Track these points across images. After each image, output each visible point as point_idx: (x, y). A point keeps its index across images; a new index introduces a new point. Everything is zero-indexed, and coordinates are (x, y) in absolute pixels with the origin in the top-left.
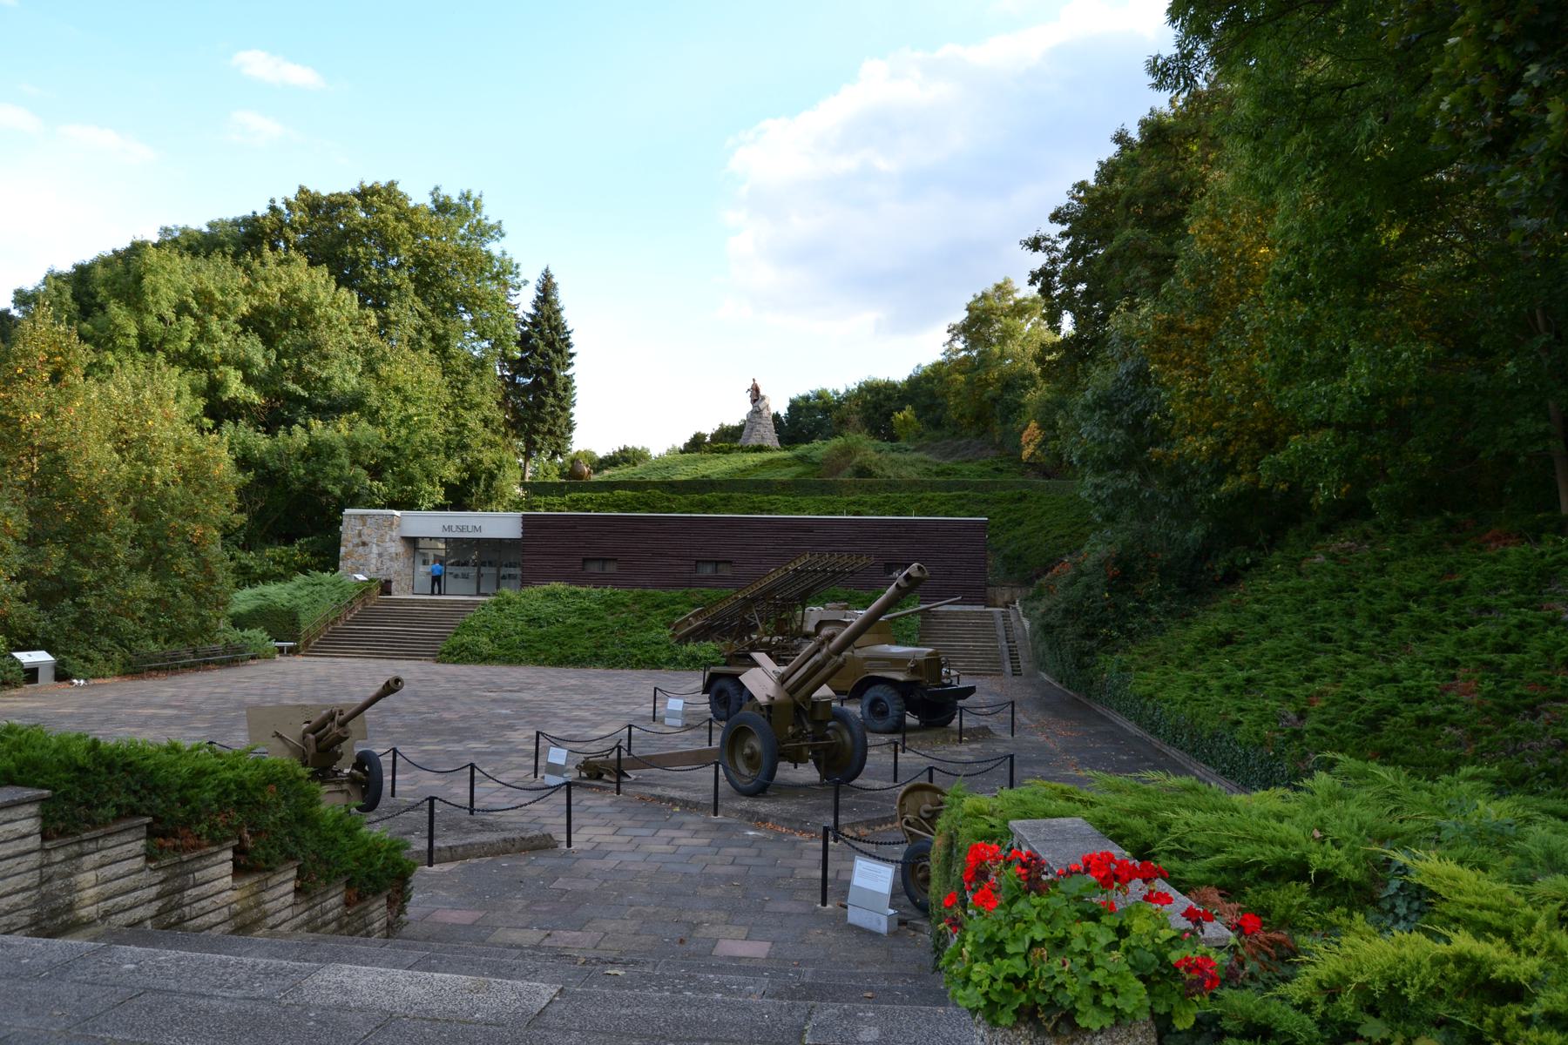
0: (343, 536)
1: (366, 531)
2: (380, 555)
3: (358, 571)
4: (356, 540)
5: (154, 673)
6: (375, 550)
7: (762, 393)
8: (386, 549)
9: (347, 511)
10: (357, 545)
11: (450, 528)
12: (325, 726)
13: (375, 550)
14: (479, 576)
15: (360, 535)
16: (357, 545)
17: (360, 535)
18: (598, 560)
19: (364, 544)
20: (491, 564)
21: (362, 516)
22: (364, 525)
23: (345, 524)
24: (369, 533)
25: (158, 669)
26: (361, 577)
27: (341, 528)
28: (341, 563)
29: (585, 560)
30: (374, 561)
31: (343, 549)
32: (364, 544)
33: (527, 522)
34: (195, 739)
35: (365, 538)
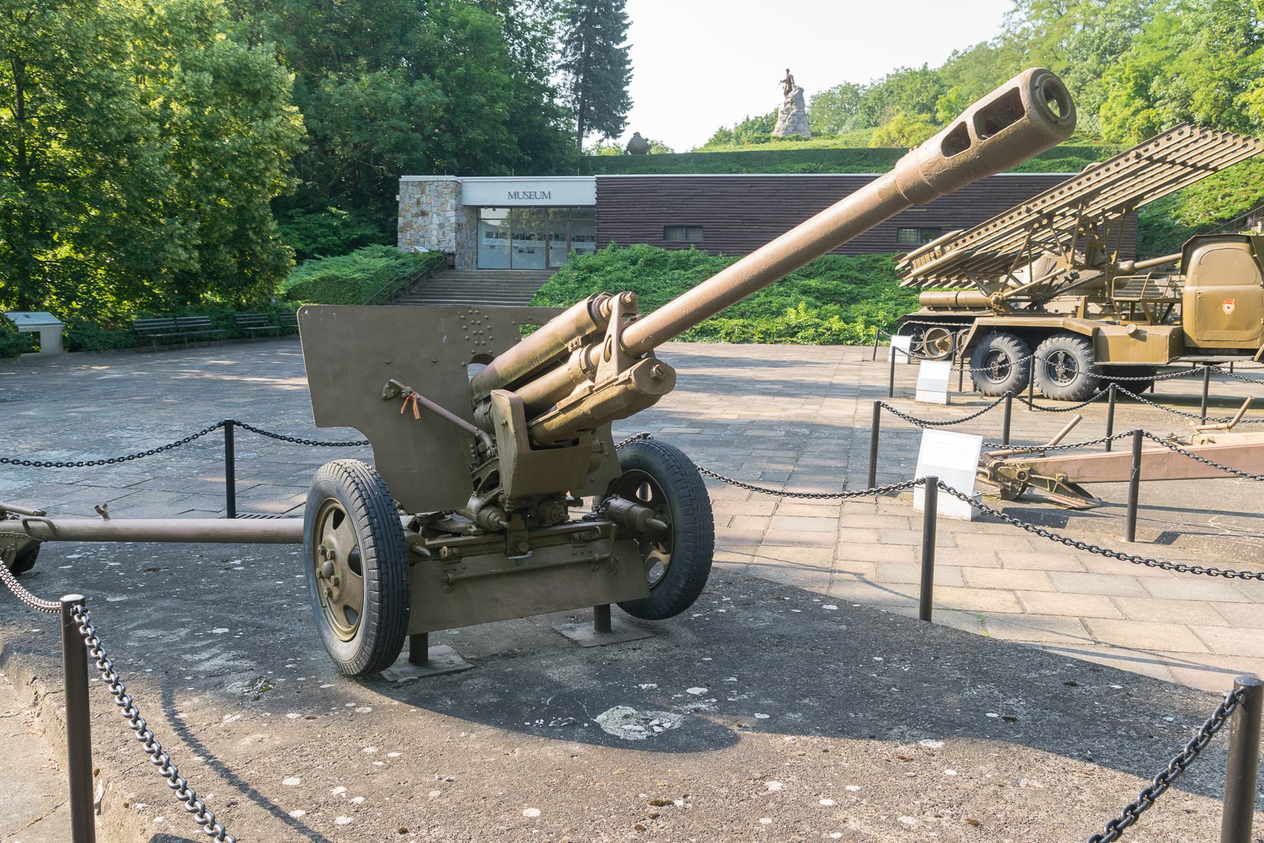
0: (401, 206)
1: (424, 200)
2: (441, 226)
3: (418, 243)
4: (415, 210)
5: (196, 343)
6: (436, 220)
7: (798, 82)
8: (447, 219)
9: (404, 178)
10: (416, 215)
11: (516, 194)
12: (564, 357)
13: (436, 220)
14: (548, 248)
15: (418, 203)
16: (416, 215)
17: (418, 203)
18: (681, 227)
19: (424, 214)
20: (557, 237)
21: (420, 182)
22: (423, 193)
23: (401, 192)
24: (428, 202)
25: (200, 339)
26: (422, 250)
27: (398, 198)
28: (399, 236)
29: (665, 227)
30: (435, 233)
31: (401, 220)
32: (424, 214)
33: (602, 188)
34: (59, 377)
35: (424, 207)
